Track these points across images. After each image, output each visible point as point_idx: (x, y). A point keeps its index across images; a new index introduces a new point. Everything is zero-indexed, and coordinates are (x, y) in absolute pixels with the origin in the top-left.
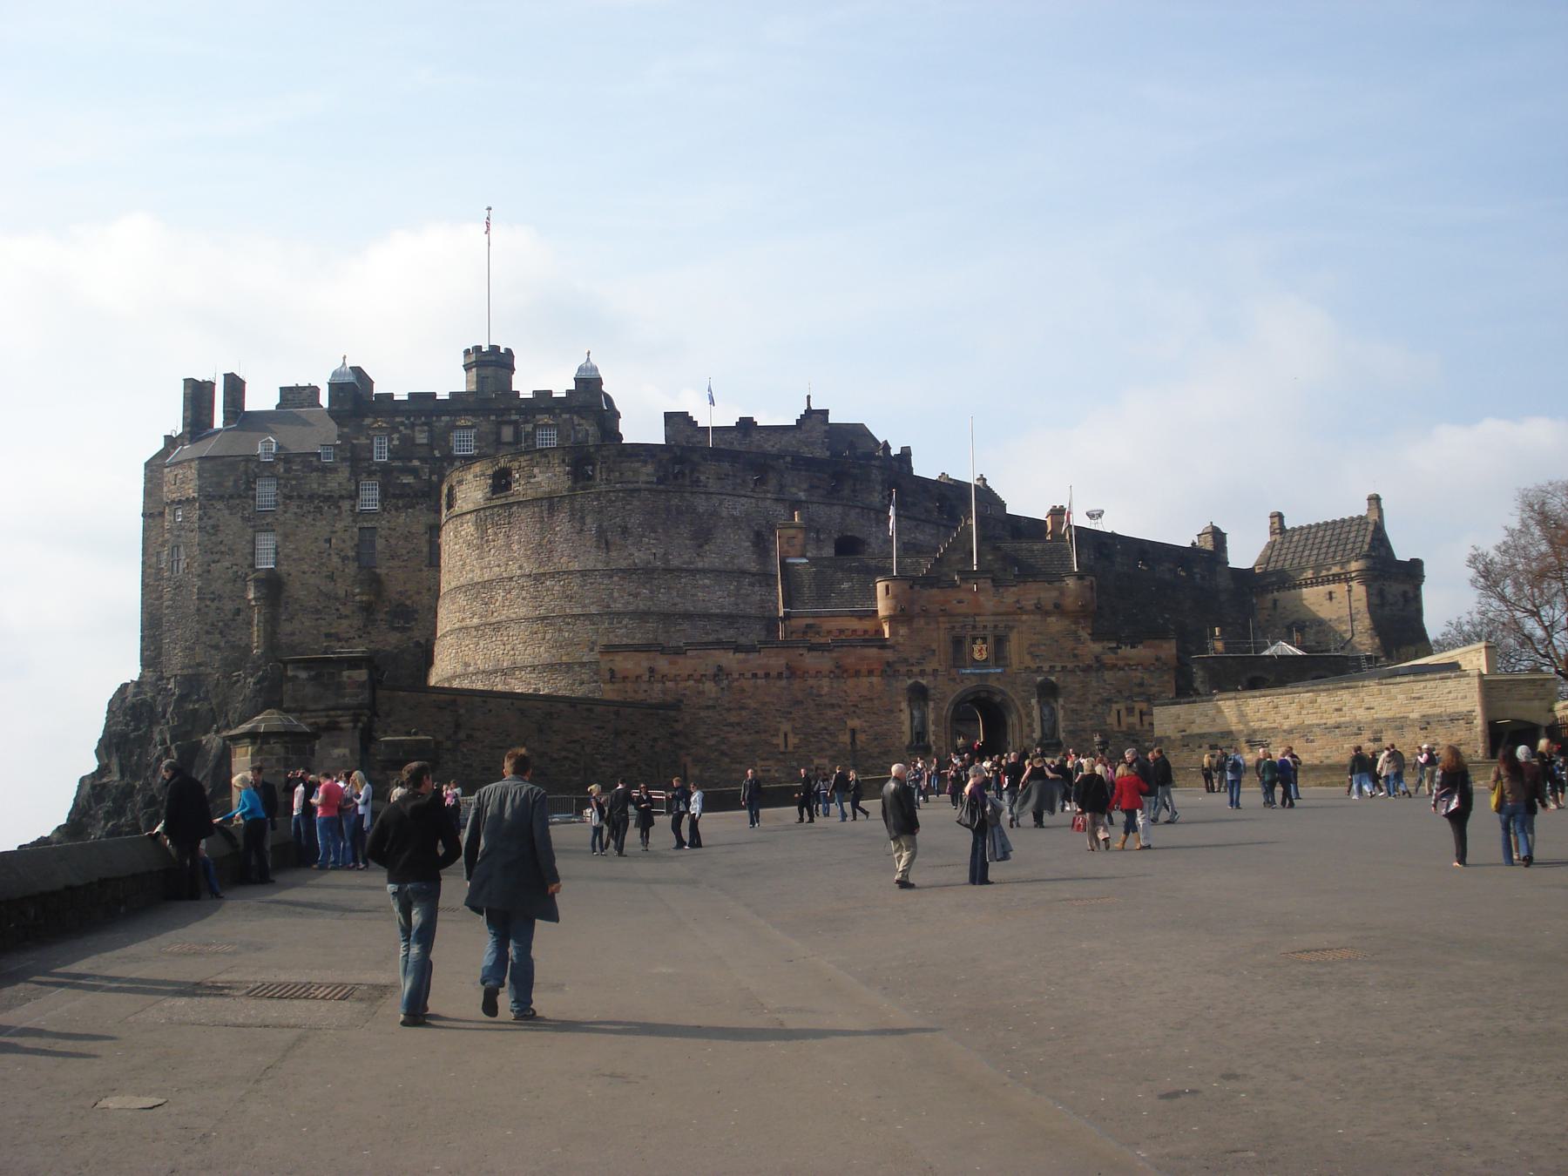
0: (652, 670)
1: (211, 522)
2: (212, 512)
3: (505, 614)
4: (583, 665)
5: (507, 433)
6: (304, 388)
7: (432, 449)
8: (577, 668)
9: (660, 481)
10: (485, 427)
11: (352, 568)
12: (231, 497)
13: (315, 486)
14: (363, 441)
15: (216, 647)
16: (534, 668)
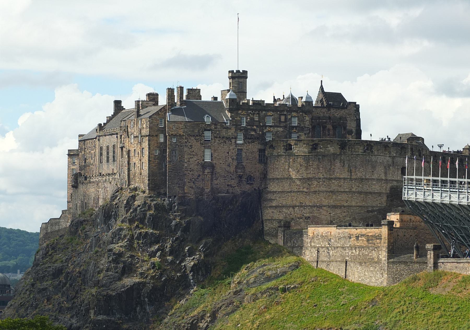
0: (410, 219)
1: (190, 144)
2: (190, 141)
3: (317, 189)
4: (344, 207)
5: (283, 118)
6: (196, 90)
7: (260, 123)
8: (343, 208)
9: (365, 152)
10: (276, 116)
11: (235, 163)
12: (197, 136)
13: (224, 134)
14: (238, 119)
15: (192, 188)
16: (329, 207)
